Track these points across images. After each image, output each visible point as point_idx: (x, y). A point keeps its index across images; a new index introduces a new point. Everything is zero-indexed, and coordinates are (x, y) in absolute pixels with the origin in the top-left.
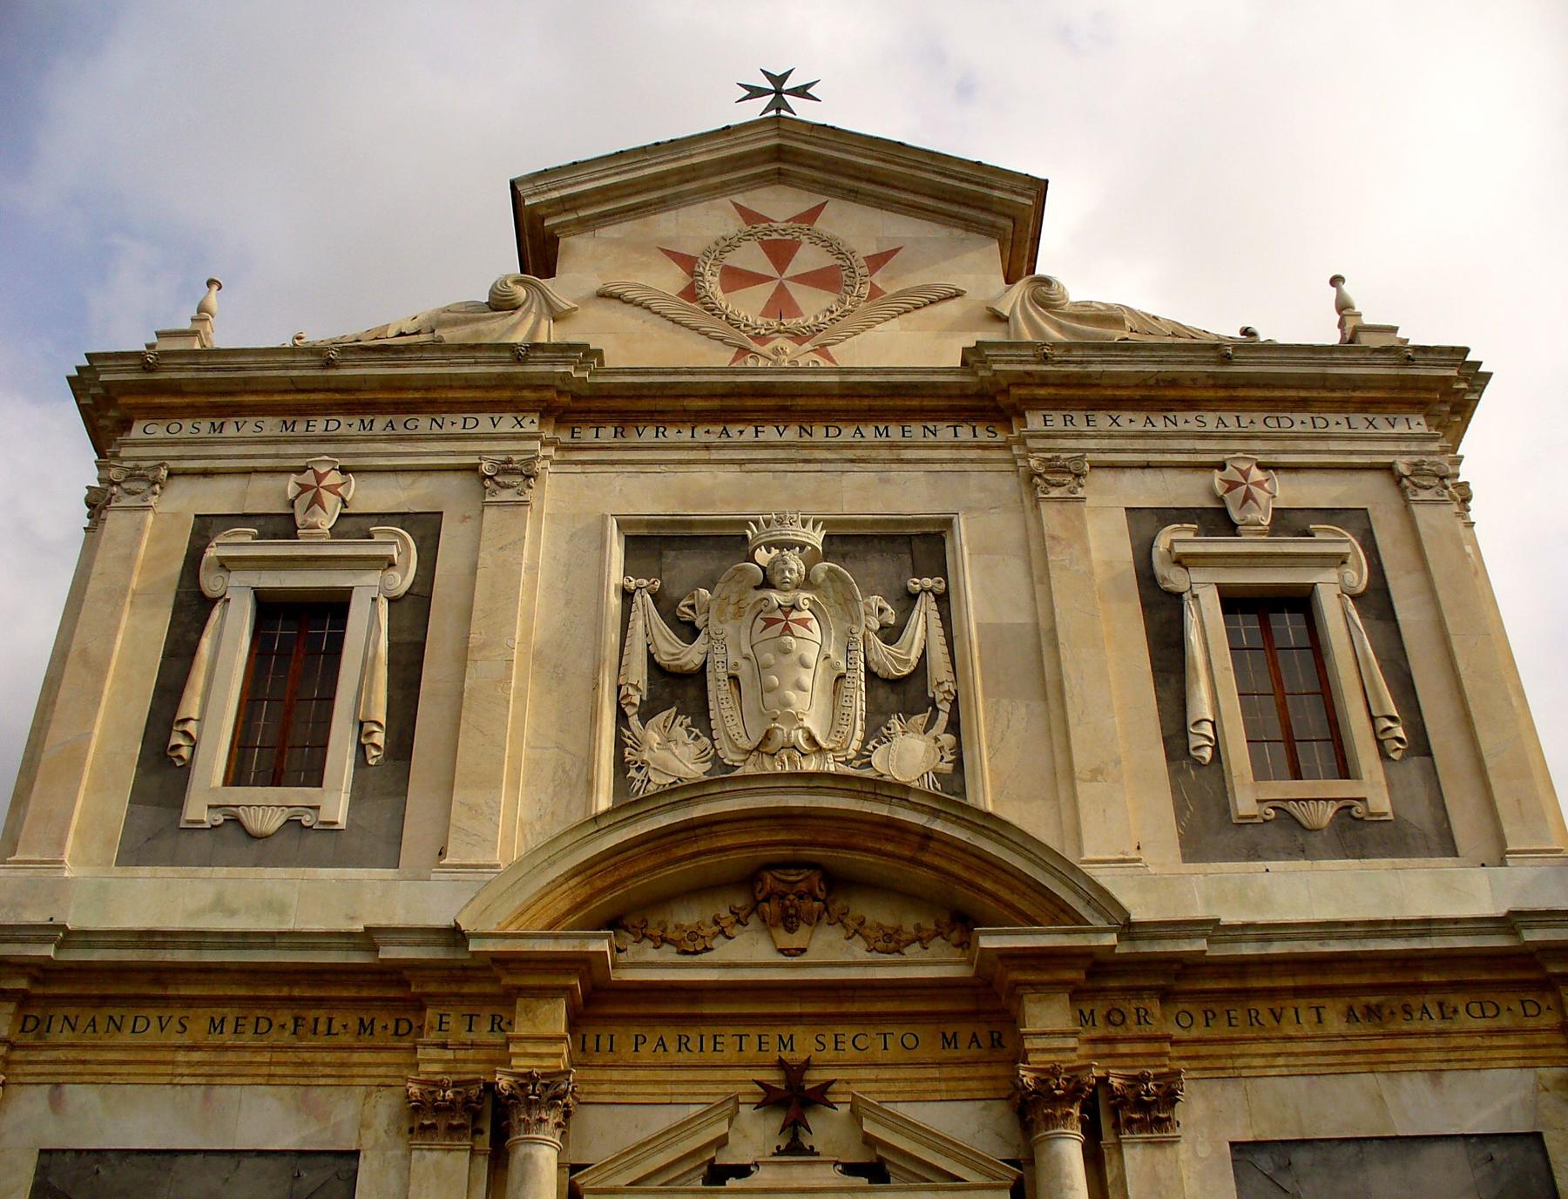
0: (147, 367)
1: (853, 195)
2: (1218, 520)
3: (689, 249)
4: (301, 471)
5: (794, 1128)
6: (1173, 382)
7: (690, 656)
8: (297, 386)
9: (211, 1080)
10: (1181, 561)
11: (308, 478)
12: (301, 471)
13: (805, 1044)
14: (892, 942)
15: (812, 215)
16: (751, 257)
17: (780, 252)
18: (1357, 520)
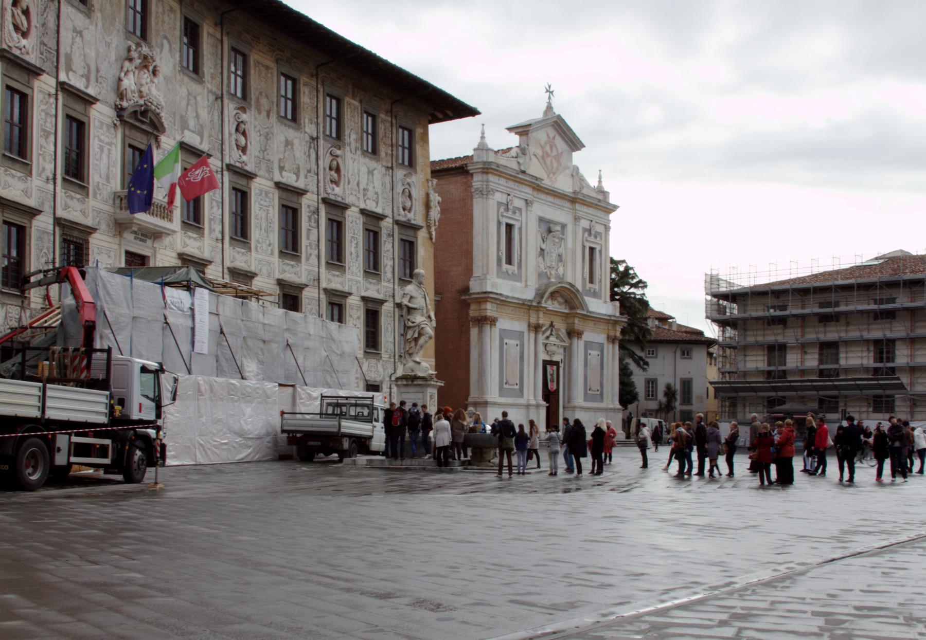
0: (498, 167)
1: (560, 134)
2: (590, 234)
3: (543, 143)
4: (509, 195)
5: (552, 331)
6: (591, 203)
7: (544, 247)
8: (511, 175)
9: (513, 319)
10: (587, 241)
11: (510, 197)
12: (509, 195)
13: (553, 318)
14: (560, 304)
15: (554, 138)
16: (548, 149)
17: (551, 147)
18: (600, 234)
